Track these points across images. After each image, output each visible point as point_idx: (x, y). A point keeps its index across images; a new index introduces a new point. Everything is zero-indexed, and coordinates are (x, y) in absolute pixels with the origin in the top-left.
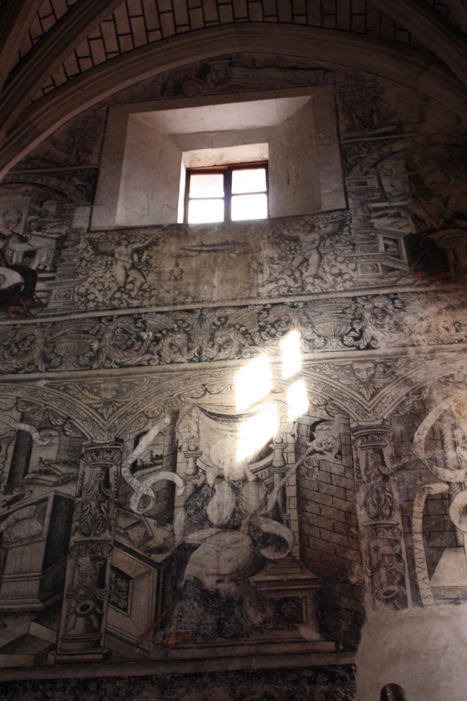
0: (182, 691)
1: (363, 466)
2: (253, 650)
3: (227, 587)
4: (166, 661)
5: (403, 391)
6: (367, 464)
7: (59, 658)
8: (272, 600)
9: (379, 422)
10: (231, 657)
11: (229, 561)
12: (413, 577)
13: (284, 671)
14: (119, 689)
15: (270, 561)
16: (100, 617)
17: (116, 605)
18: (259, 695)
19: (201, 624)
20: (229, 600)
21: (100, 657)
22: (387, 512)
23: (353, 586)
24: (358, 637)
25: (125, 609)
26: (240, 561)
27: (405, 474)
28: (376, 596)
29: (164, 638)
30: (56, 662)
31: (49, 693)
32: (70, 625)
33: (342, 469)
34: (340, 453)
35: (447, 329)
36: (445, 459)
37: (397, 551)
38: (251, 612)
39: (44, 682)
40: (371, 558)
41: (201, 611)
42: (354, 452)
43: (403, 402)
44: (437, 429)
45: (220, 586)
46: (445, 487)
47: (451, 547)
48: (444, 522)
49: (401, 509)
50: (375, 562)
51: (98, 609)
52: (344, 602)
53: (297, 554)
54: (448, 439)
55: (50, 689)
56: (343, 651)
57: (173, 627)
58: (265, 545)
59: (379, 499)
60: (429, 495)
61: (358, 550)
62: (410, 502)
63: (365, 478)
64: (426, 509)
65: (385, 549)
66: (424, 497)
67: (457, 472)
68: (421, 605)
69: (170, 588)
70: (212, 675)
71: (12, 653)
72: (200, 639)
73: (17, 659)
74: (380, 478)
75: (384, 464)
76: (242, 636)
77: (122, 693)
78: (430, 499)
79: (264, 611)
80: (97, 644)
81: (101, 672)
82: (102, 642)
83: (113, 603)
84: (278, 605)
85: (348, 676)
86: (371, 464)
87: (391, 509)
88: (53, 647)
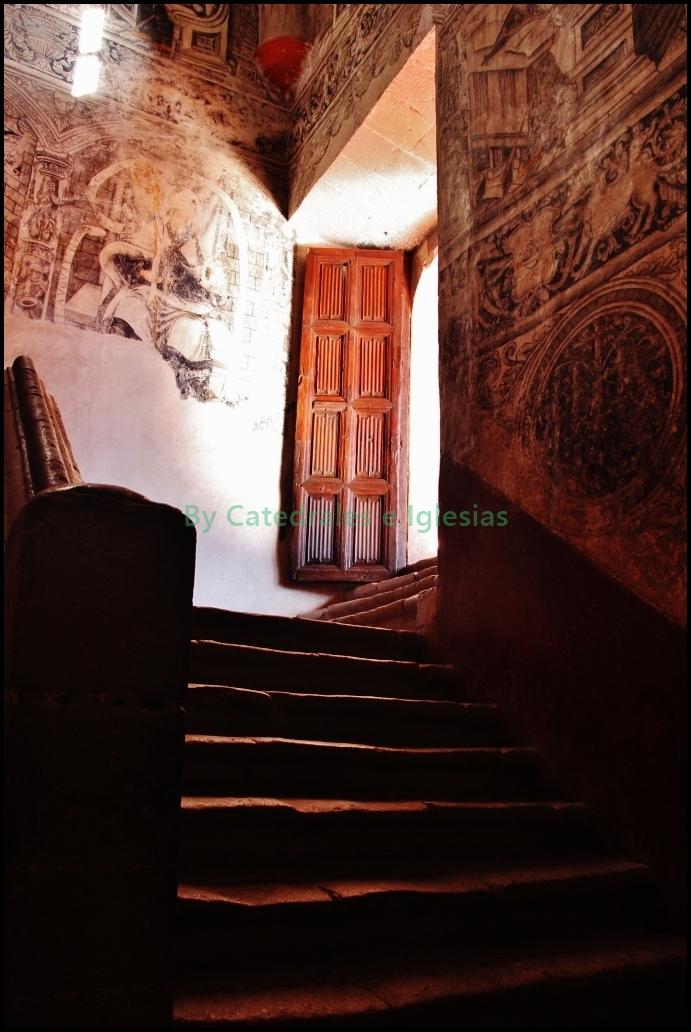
1: (37, 189)
5: (94, 137)
6: (42, 188)
9: (64, 156)
12: (53, 297)
22: (47, 236)
27: (72, 210)
33: (17, 184)
34: (19, 169)
35: (150, 99)
36: (111, 209)
37: (46, 272)
40: (21, 269)
42: (33, 174)
43: (90, 147)
44: (112, 181)
46: (102, 233)
47: (91, 282)
49: (60, 238)
50: (23, 274)
54: (119, 194)
59: (43, 222)
62: (70, 234)
63: (36, 200)
64: (81, 246)
66: (83, 234)
67: (117, 223)
68: (53, 321)
74: (49, 205)
75: (57, 194)
78: (86, 238)
86: (45, 190)
87: (51, 234)
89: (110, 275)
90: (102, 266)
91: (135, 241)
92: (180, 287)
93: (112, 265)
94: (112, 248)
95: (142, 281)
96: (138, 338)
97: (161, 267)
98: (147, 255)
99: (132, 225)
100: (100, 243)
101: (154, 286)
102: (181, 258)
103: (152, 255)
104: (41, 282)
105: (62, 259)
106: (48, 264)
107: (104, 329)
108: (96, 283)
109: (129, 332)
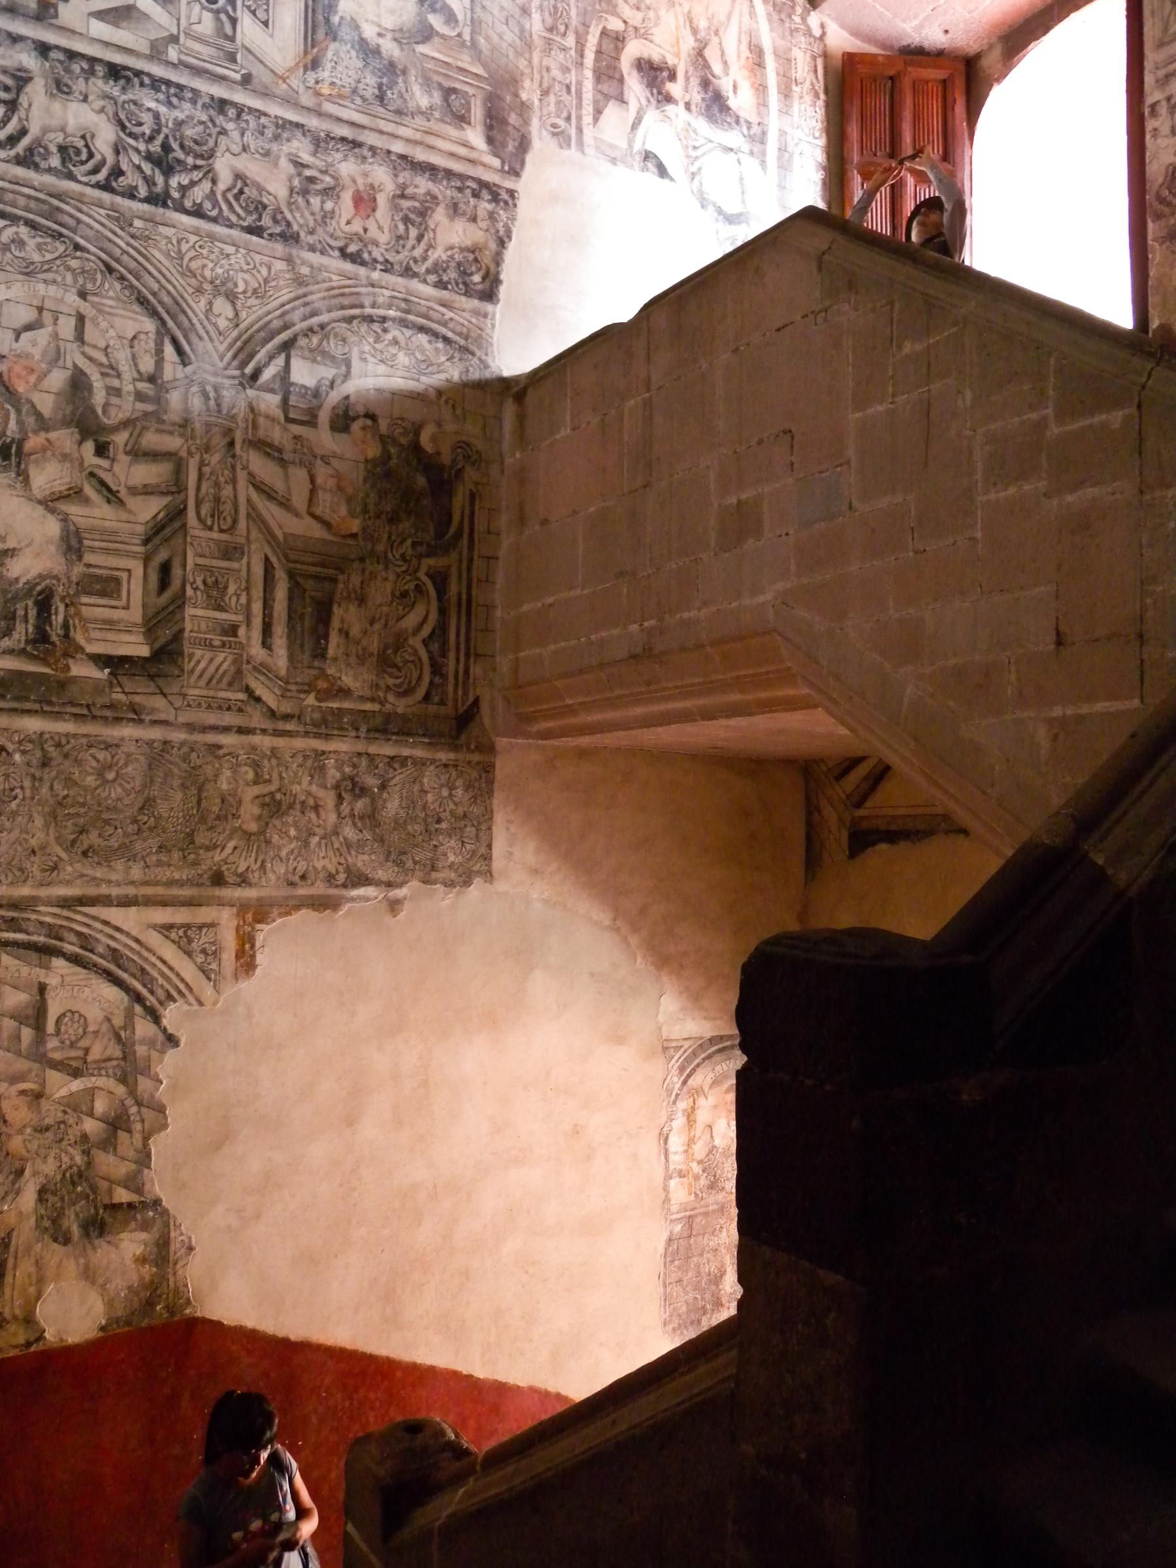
0: (339, 156)
2: (418, 136)
3: (389, 48)
4: (320, 114)
7: (183, 57)
8: (440, 84)
10: (395, 136)
11: (392, 12)
12: (579, 118)
13: (449, 174)
14: (264, 127)
15: (438, 33)
16: (234, 21)
17: (254, 13)
18: (421, 191)
19: (359, 82)
20: (392, 65)
21: (238, 77)
22: (562, 28)
23: (523, 103)
24: (523, 163)
25: (266, 24)
26: (405, 18)
28: (543, 125)
29: (317, 82)
30: (181, 62)
31: (174, 100)
32: (194, 19)
37: (568, 82)
38: (416, 88)
39: (168, 83)
40: (542, 77)
41: (360, 64)
45: (381, 41)
47: (616, 99)
48: (615, 68)
49: (577, 33)
50: (545, 85)
51: (229, 9)
52: (513, 119)
53: (467, 37)
55: (176, 95)
56: (508, 173)
57: (326, 74)
58: (434, 11)
59: (555, 7)
60: (604, 28)
61: (530, 61)
64: (600, 44)
65: (556, 73)
66: (600, 27)
67: (635, 12)
68: (583, 152)
69: (320, 17)
70: (372, 149)
71: (115, 24)
72: (358, 101)
73: (122, 36)
76: (406, 115)
77: (269, 133)
78: (604, 33)
79: (431, 96)
80: (232, 58)
81: (240, 97)
82: (239, 57)
83: (249, 7)
84: (448, 92)
85: (511, 202)
88: (174, 39)
89: (635, 87)
90: (626, 76)
91: (657, 39)
92: (708, 108)
93: (635, 73)
94: (633, 49)
95: (669, 99)
96: (672, 179)
97: (687, 79)
98: (671, 61)
99: (651, 14)
100: (619, 40)
101: (681, 105)
102: (706, 66)
103: (676, 61)
104: (566, 98)
105: (582, 64)
106: (568, 70)
107: (636, 164)
108: (621, 100)
109: (662, 171)
